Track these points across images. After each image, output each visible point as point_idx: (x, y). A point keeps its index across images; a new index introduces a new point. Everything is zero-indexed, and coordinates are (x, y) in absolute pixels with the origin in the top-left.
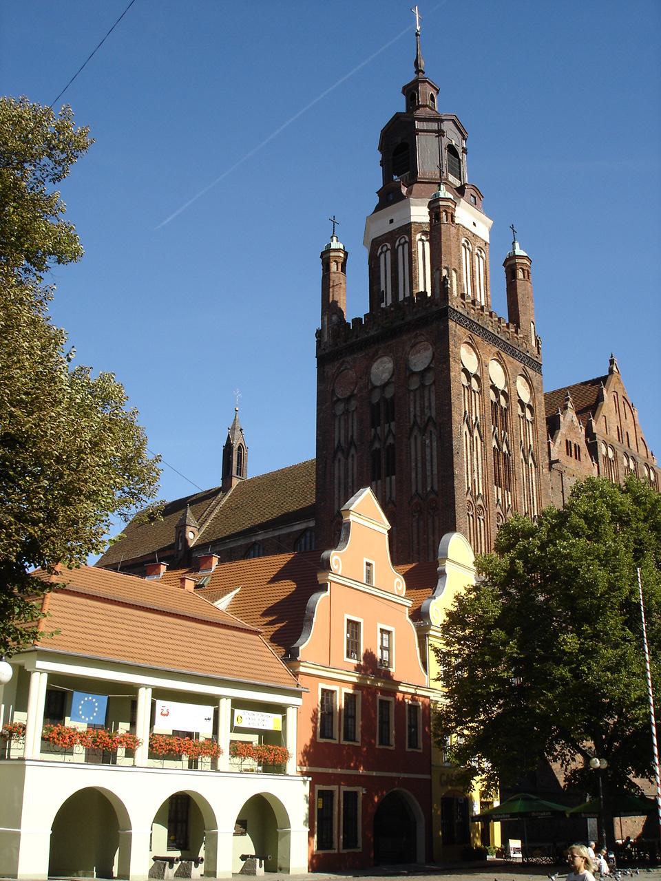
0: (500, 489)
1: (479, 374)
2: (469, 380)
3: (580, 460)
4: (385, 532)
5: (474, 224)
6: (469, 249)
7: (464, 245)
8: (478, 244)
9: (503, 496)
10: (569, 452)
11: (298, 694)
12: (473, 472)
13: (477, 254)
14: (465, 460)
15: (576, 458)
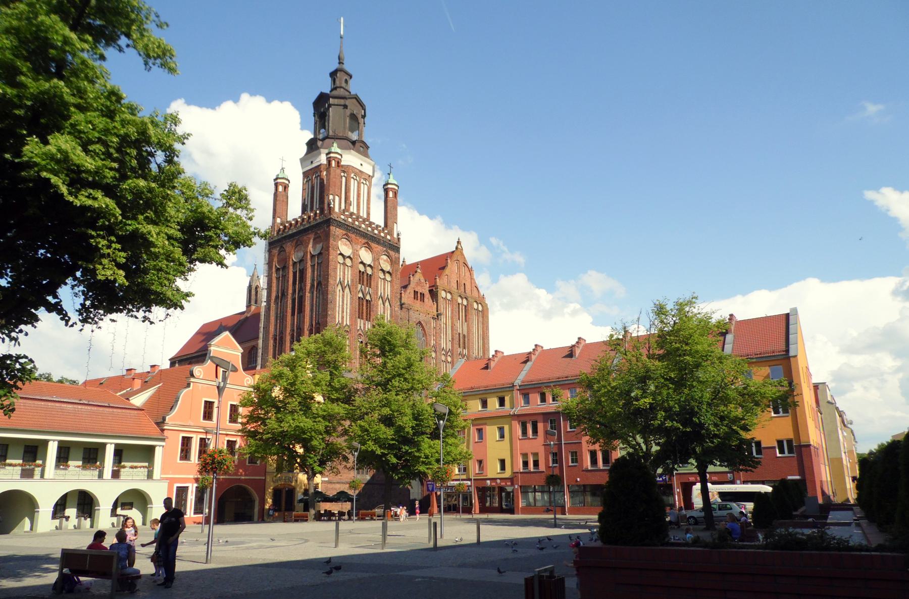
0: (362, 321)
1: (352, 256)
2: (344, 259)
3: (423, 301)
4: (240, 354)
5: (361, 165)
6: (356, 180)
7: (353, 178)
8: (363, 177)
9: (365, 324)
10: (415, 297)
11: (163, 440)
12: (343, 312)
13: (363, 183)
14: (338, 305)
15: (421, 301)
